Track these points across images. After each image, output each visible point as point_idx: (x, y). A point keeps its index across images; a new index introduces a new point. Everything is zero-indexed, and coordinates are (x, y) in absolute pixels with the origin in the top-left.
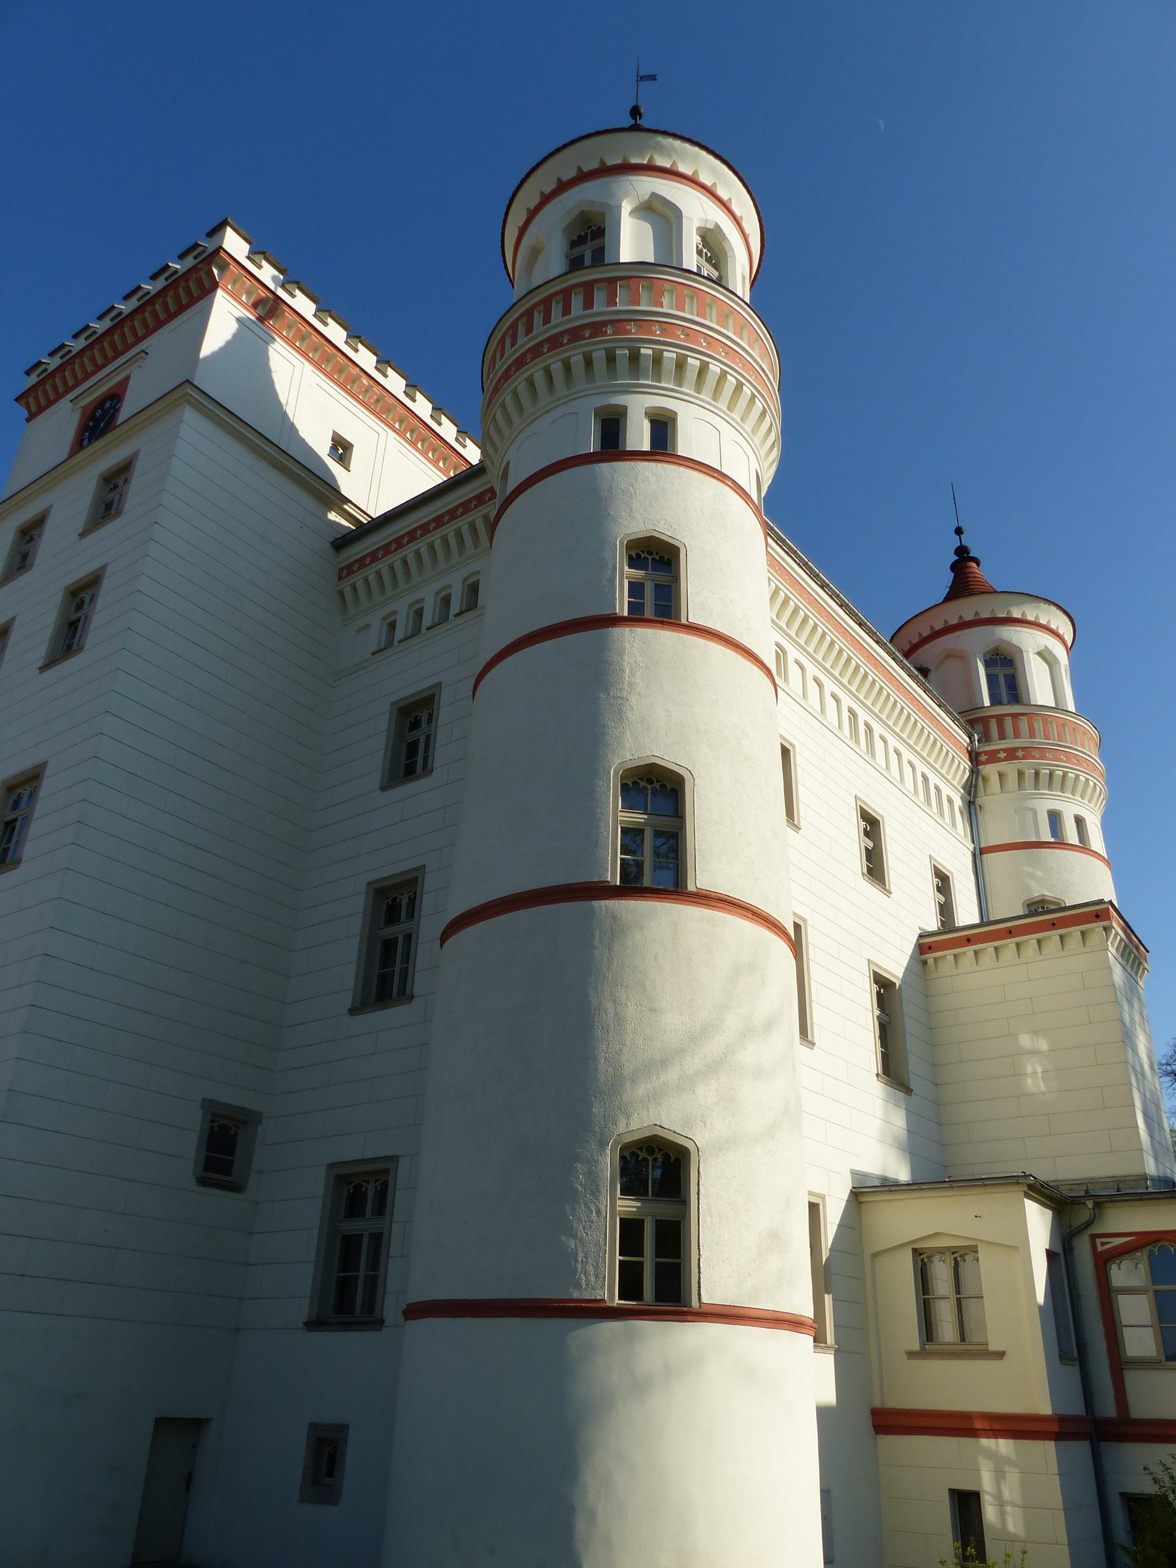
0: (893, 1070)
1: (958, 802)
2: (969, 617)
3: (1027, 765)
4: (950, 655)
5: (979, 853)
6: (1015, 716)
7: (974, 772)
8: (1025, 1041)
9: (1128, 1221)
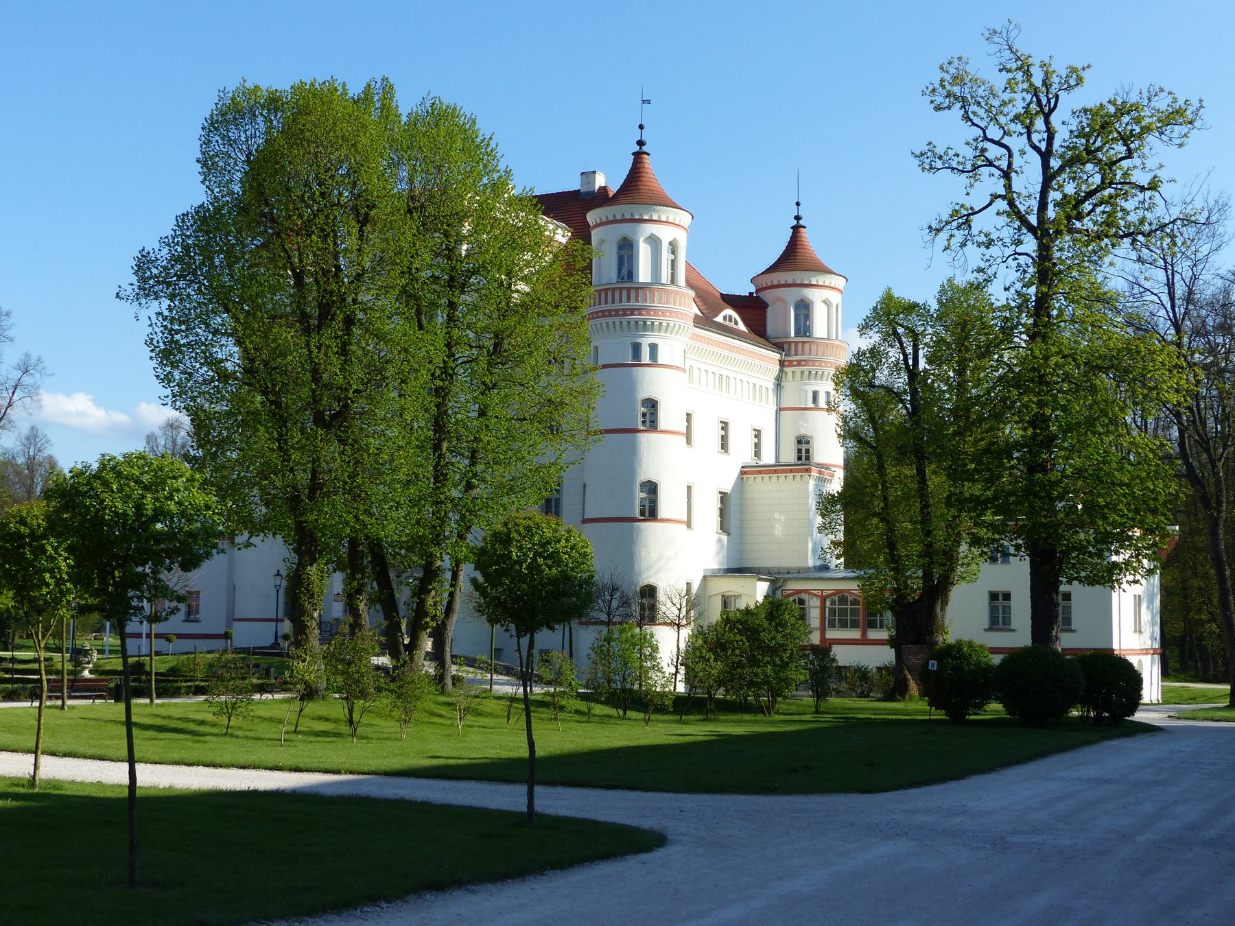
0: (724, 527)
1: (771, 386)
2: (790, 282)
3: (806, 369)
4: (779, 299)
5: (780, 410)
6: (804, 343)
7: (781, 371)
8: (777, 516)
9: (793, 586)
